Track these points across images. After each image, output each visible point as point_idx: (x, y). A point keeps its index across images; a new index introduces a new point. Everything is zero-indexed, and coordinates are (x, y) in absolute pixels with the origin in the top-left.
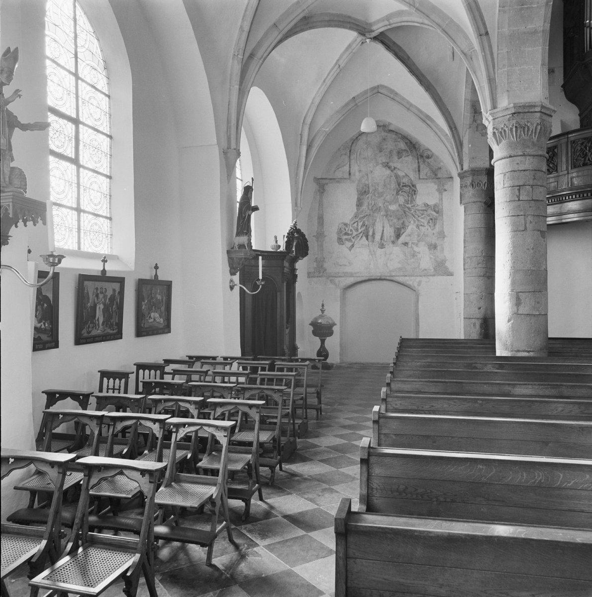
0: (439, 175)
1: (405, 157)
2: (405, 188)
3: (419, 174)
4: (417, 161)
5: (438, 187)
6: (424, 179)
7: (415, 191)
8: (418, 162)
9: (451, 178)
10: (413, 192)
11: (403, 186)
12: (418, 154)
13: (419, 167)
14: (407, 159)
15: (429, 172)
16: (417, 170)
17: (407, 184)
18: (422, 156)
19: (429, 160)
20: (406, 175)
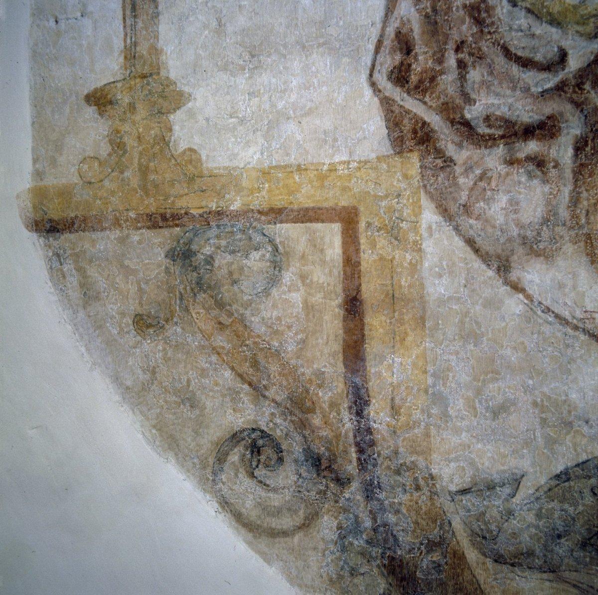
0: (151, 251)
1: (517, 482)
2: (526, 112)
3: (351, 265)
4: (379, 415)
5: (163, 141)
6: (308, 216)
7: (400, 76)
8: (359, 403)
9: (49, 227)
10: (422, 61)
11: (545, 129)
12: (370, 490)
13: (354, 352)
14: (491, 458)
15: (247, 288)
16: (376, 323)
17: (493, 159)
18: (321, 464)
19: (245, 414)
20: (503, 267)
